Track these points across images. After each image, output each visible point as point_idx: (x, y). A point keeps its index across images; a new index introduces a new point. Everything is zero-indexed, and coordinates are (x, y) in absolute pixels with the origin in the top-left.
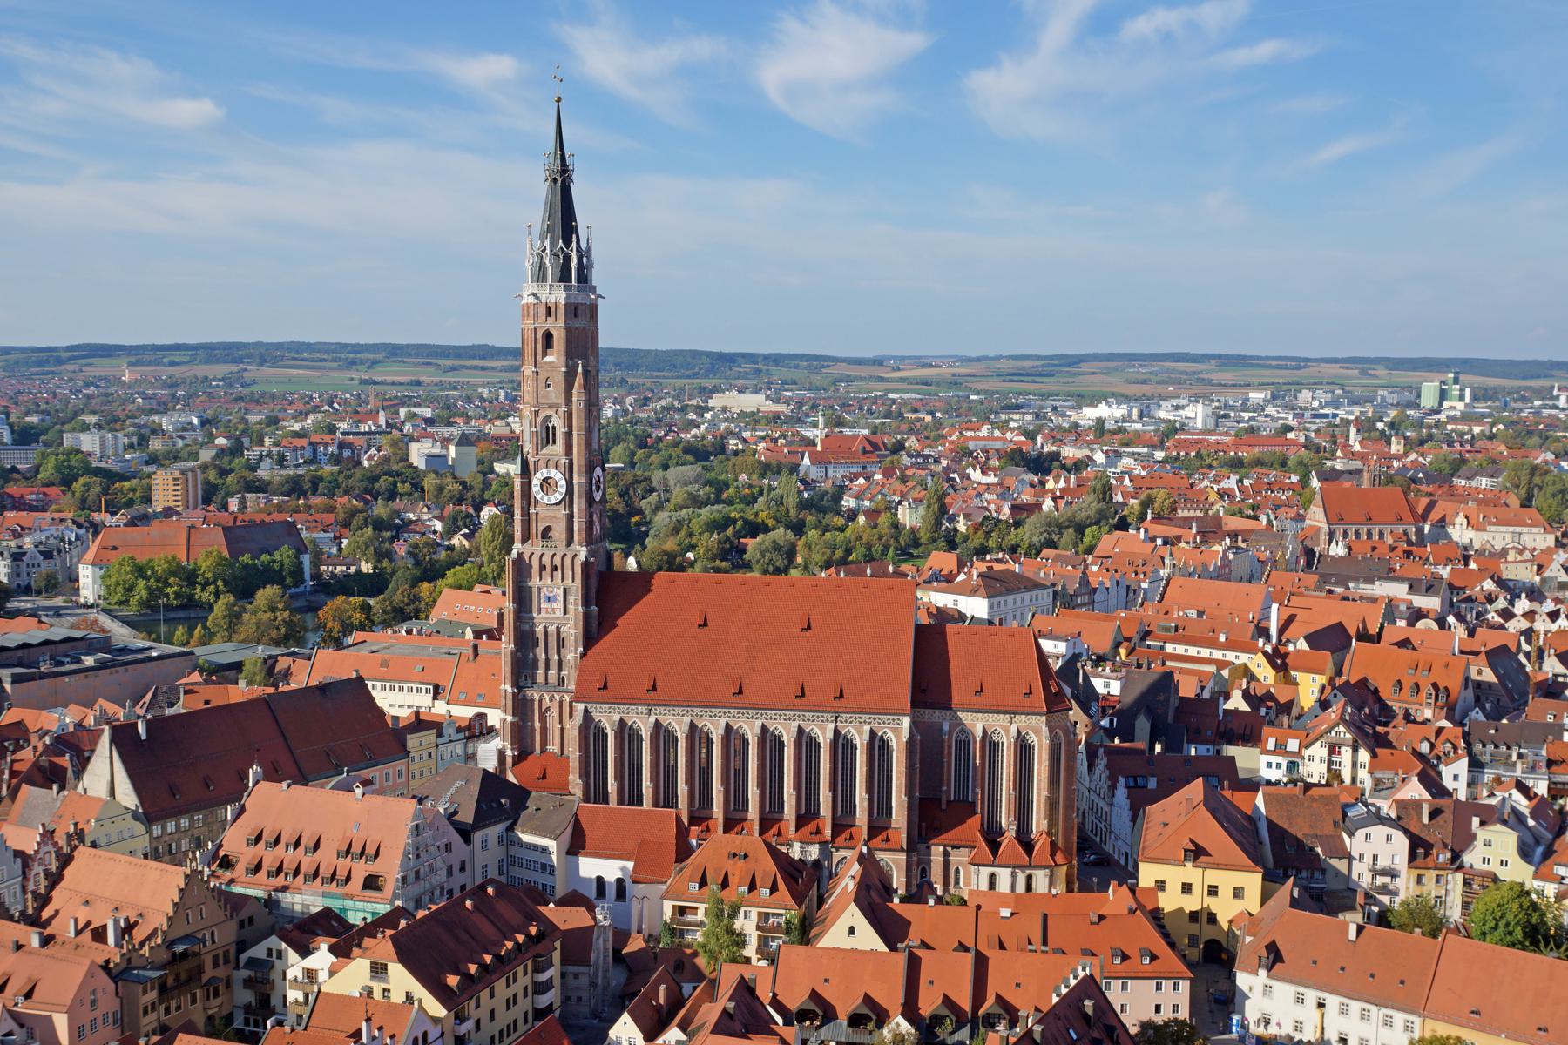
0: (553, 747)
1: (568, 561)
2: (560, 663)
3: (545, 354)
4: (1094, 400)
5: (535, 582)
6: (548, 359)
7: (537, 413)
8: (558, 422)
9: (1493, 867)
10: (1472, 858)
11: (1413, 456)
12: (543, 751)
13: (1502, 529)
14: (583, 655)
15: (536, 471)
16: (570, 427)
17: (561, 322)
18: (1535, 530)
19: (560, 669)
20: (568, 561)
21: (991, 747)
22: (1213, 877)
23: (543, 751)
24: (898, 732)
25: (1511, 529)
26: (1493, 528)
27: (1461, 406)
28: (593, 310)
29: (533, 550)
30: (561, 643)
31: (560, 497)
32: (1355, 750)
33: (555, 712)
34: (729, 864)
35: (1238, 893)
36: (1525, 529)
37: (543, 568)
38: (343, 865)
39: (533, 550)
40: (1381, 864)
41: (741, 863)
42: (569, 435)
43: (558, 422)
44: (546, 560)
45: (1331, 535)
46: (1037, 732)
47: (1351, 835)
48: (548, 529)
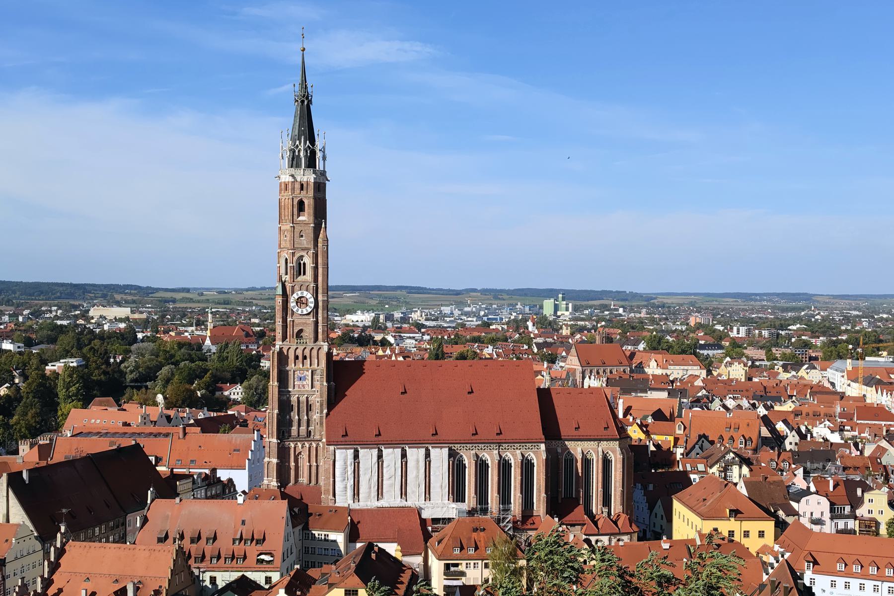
0: (303, 479)
1: (314, 352)
2: (308, 421)
3: (299, 216)
4: (352, 311)
5: (291, 366)
6: (301, 218)
7: (293, 254)
8: (308, 261)
9: (875, 515)
10: (861, 512)
11: (578, 336)
12: (296, 481)
13: (677, 367)
14: (328, 414)
15: (293, 293)
16: (317, 263)
17: (311, 193)
18: (695, 368)
19: (308, 426)
20: (314, 352)
21: (587, 462)
22: (747, 525)
23: (296, 481)
24: (538, 455)
25: (682, 367)
26: (672, 367)
27: (567, 313)
29: (291, 347)
30: (309, 408)
31: (310, 310)
32: (741, 468)
33: (305, 455)
34: (475, 535)
35: (761, 534)
36: (690, 367)
37: (297, 358)
38: (239, 548)
39: (291, 347)
40: (815, 516)
41: (482, 534)
42: (316, 268)
43: (308, 261)
44: (299, 352)
45: (583, 373)
46: (614, 452)
47: (798, 501)
48: (301, 331)
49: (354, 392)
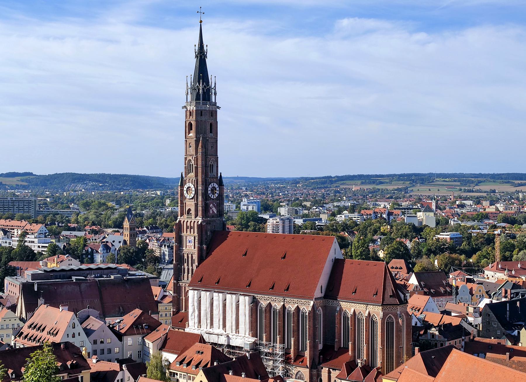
3: (189, 133)
5: (184, 234)
6: (191, 135)
16: (197, 164)
28: (213, 114)
37: (187, 227)
42: (197, 168)
49: (217, 253)
